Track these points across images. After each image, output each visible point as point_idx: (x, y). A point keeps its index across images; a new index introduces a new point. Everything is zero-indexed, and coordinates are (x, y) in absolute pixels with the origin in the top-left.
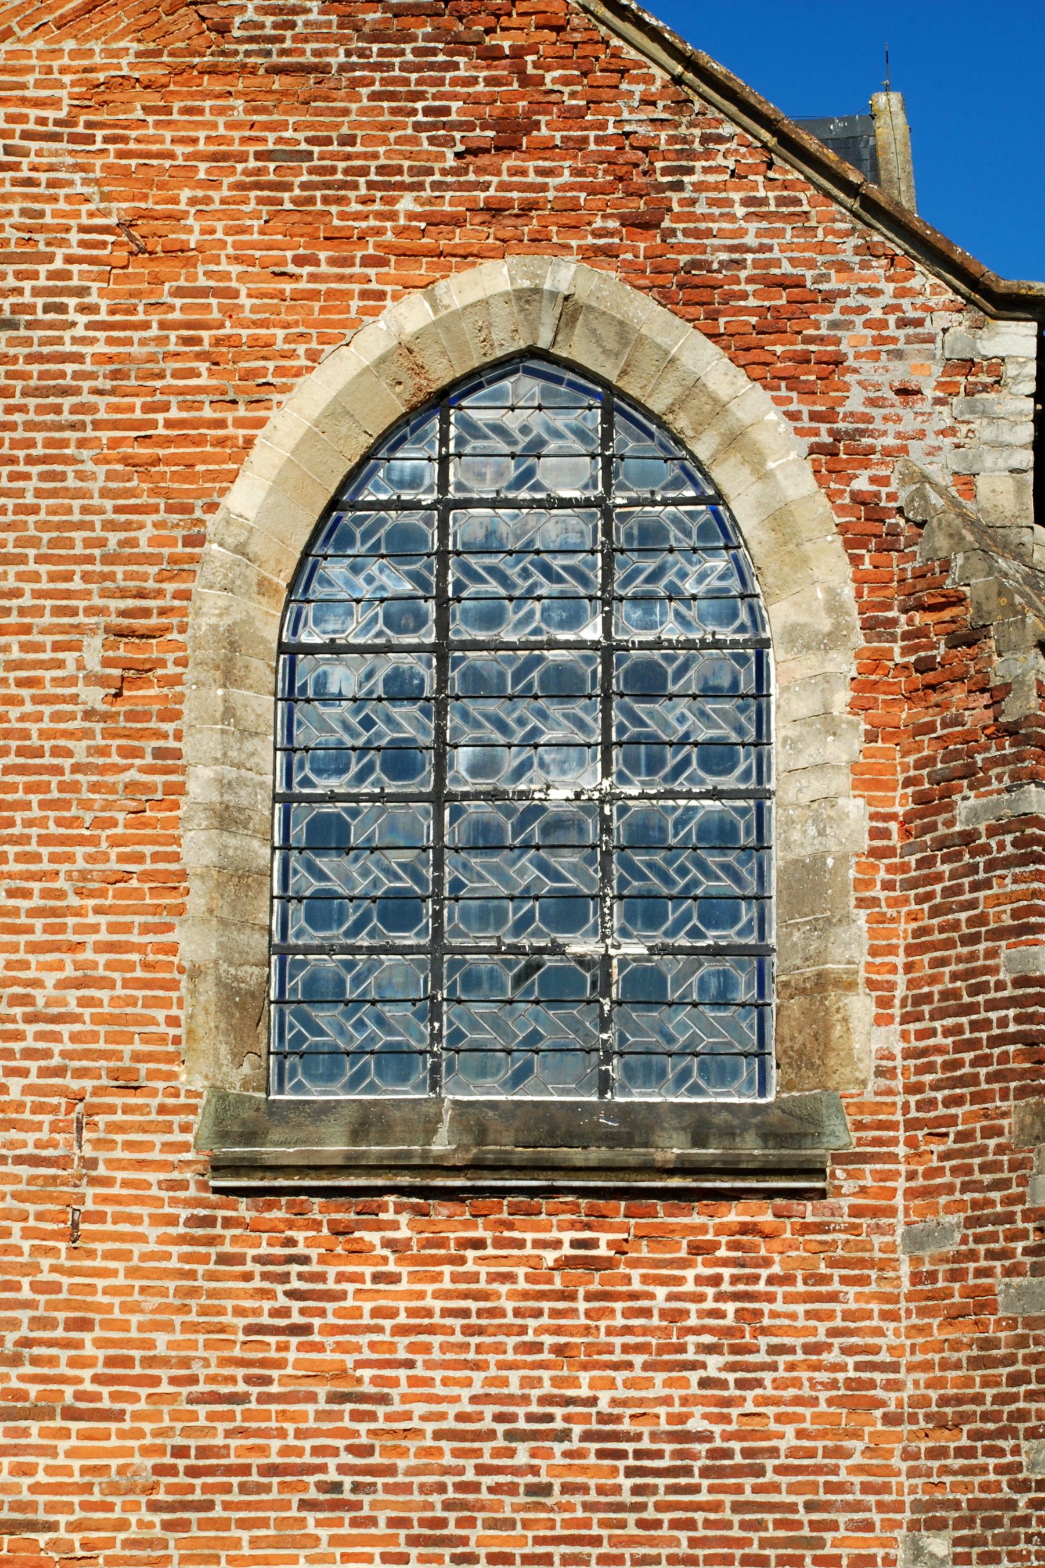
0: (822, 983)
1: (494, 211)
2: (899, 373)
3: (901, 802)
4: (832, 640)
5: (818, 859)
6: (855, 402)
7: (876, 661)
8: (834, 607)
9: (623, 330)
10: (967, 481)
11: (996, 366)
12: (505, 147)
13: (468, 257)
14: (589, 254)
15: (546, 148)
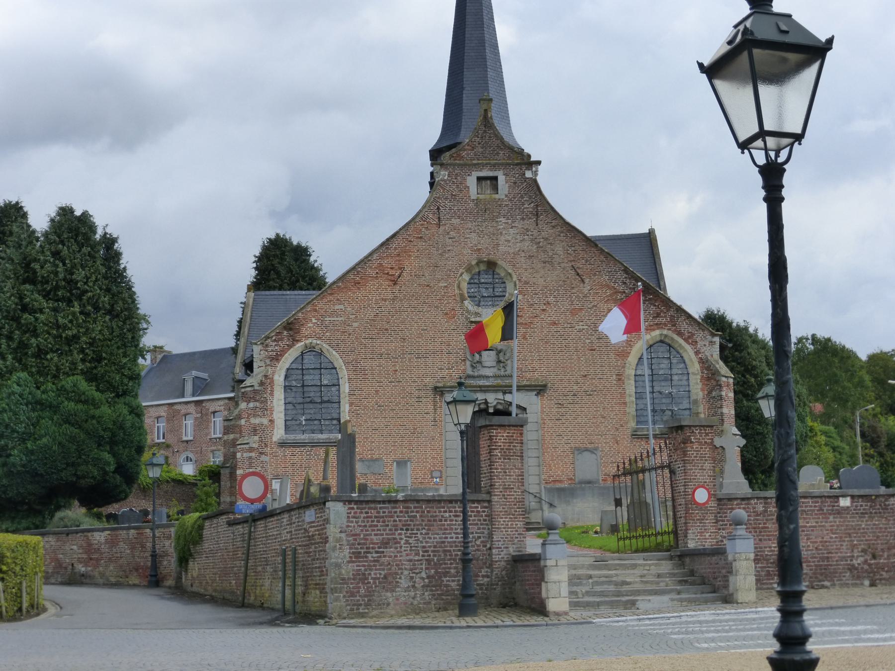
0: (698, 413)
1: (657, 324)
2: (704, 343)
3: (706, 392)
4: (698, 374)
5: (697, 400)
6: (699, 346)
7: (702, 377)
8: (698, 370)
9: (672, 339)
10: (712, 356)
11: (715, 342)
12: (657, 317)
13: (654, 330)
14: (668, 329)
15: (662, 317)
